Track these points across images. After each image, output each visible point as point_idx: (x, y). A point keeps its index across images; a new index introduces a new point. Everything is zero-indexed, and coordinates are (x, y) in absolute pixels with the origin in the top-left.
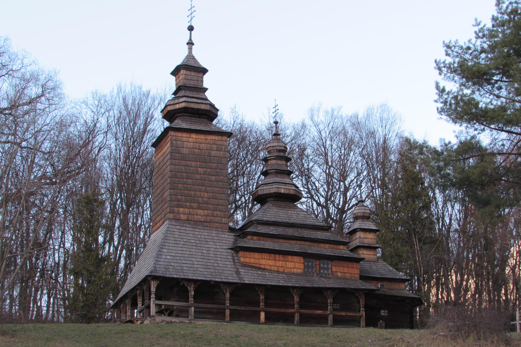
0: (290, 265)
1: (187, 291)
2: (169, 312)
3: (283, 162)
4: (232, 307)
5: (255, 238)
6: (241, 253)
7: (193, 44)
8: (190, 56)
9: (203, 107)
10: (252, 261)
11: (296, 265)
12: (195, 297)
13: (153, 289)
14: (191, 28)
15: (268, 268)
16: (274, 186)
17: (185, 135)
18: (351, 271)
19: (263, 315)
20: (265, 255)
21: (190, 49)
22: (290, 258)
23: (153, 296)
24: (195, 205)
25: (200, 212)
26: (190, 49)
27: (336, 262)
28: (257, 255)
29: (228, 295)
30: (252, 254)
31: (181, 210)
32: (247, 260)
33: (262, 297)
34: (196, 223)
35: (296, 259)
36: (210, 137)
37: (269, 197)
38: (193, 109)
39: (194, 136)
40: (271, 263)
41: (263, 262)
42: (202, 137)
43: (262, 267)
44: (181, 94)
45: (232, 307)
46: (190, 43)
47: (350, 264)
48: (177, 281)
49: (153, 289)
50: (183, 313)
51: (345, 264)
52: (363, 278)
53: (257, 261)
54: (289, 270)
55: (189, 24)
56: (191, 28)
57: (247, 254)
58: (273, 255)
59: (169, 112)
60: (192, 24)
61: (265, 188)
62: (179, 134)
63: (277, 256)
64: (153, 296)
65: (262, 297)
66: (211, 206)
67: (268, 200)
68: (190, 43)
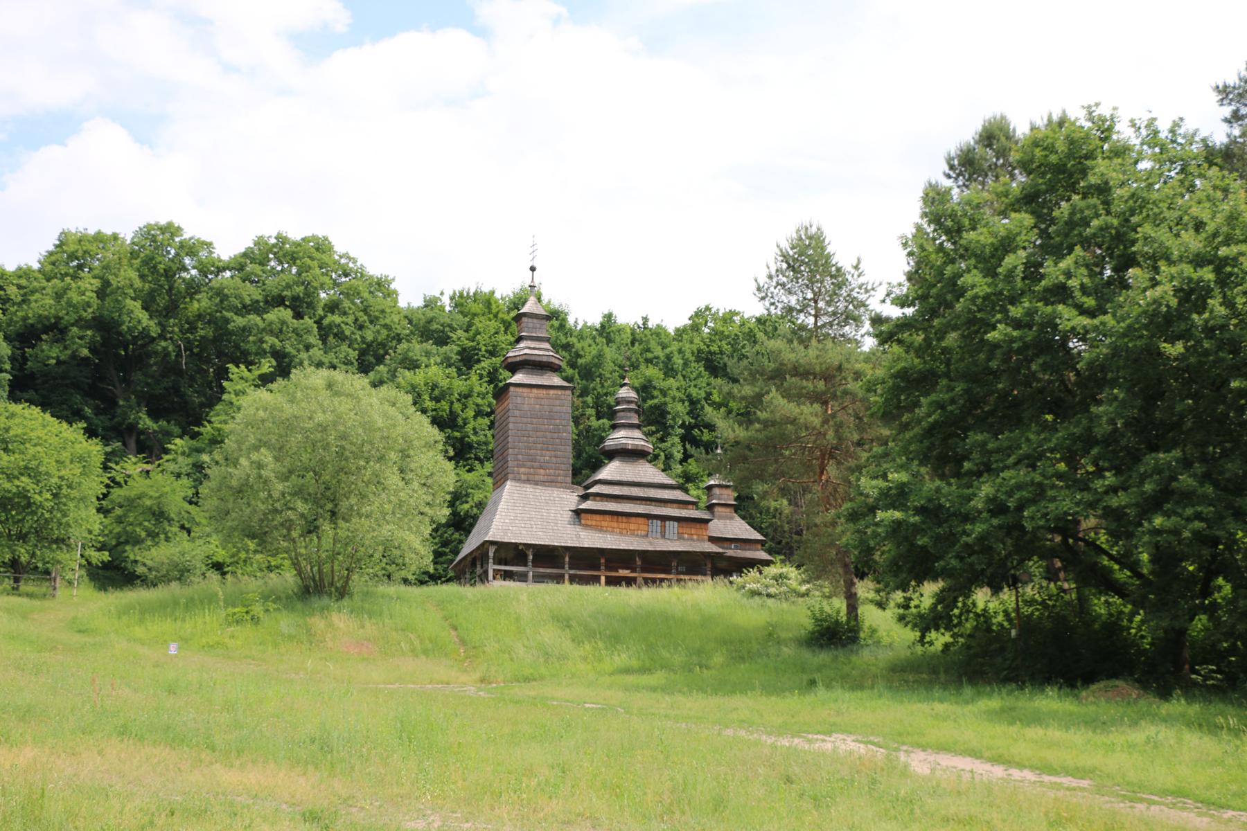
1: (526, 556)
2: (508, 576)
4: (572, 572)
6: (583, 515)
12: (533, 561)
13: (491, 554)
14: (533, 269)
19: (603, 579)
20: (608, 518)
22: (633, 519)
23: (491, 561)
24: (536, 464)
25: (542, 471)
27: (684, 524)
28: (598, 517)
29: (567, 559)
30: (594, 516)
31: (522, 470)
32: (589, 523)
33: (603, 561)
35: (640, 520)
36: (552, 392)
39: (535, 391)
42: (544, 392)
44: (522, 344)
45: (572, 572)
48: (515, 544)
49: (491, 554)
50: (522, 577)
51: (693, 525)
52: (713, 540)
56: (533, 269)
57: (589, 516)
64: (491, 561)
65: (603, 561)
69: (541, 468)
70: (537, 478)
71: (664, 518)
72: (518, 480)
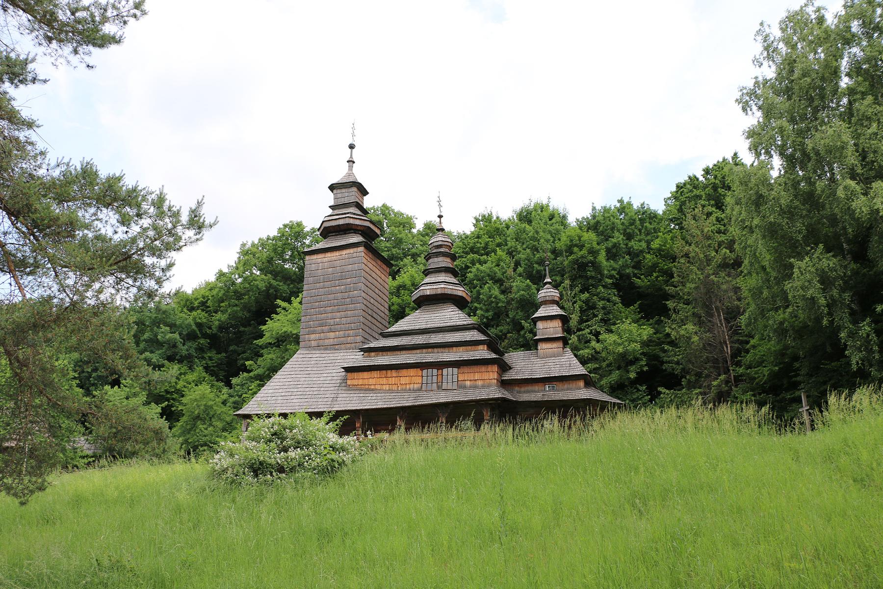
0: (404, 380)
3: (448, 260)
5: (373, 354)
8: (350, 173)
9: (341, 222)
10: (360, 382)
11: (412, 379)
14: (352, 147)
15: (378, 387)
17: (320, 256)
18: (486, 376)
20: (375, 374)
21: (351, 168)
22: (404, 372)
25: (332, 335)
26: (351, 168)
27: (465, 369)
28: (366, 375)
31: (313, 336)
32: (355, 382)
34: (326, 348)
35: (412, 372)
36: (344, 252)
40: (384, 381)
42: (337, 253)
43: (373, 387)
46: (351, 162)
47: (483, 368)
53: (366, 382)
54: (404, 387)
56: (352, 147)
58: (384, 372)
62: (314, 257)
63: (389, 371)
69: (331, 331)
70: (327, 342)
71: (440, 365)
72: (309, 347)
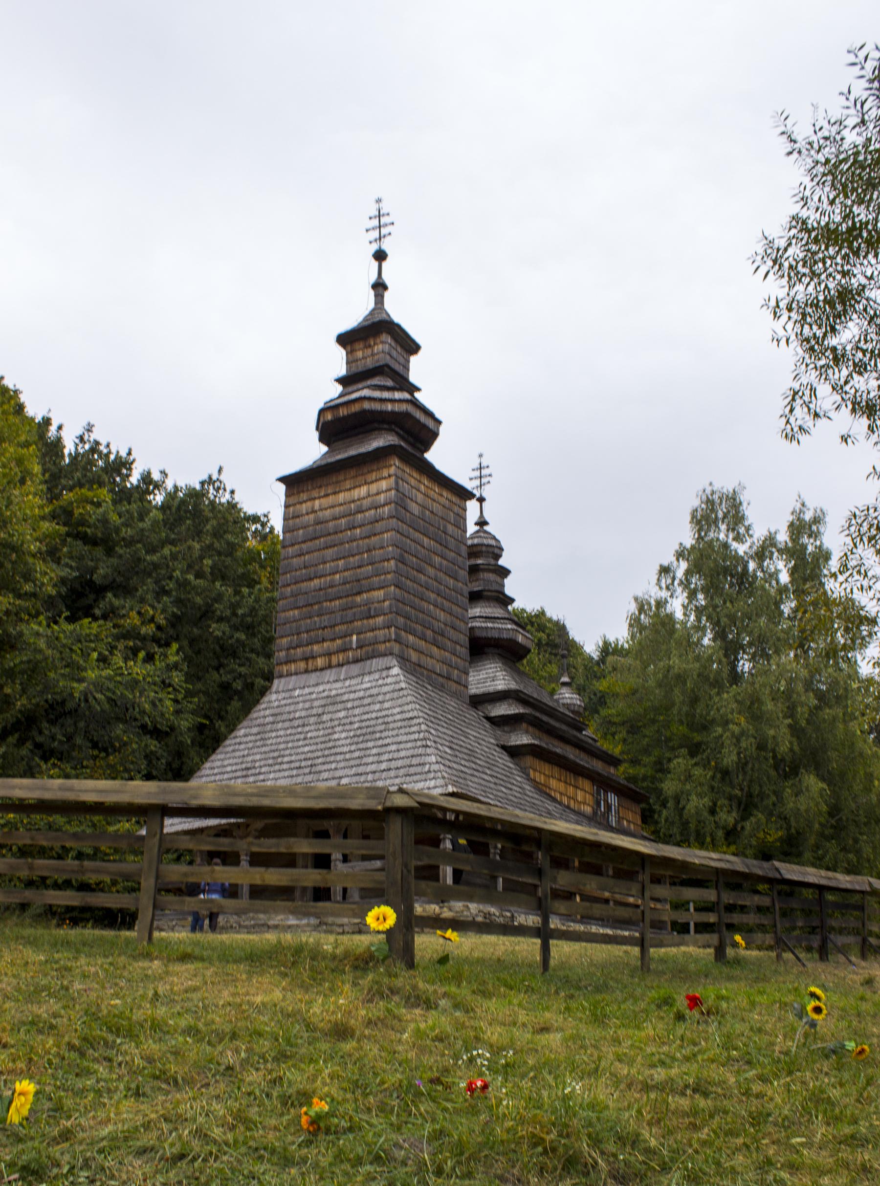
7: (385, 288)
14: (380, 256)
16: (509, 626)
28: (547, 768)
37: (489, 646)
38: (418, 421)
41: (553, 783)
46: (379, 287)
55: (375, 247)
56: (380, 256)
59: (364, 412)
60: (384, 247)
61: (490, 625)
66: (449, 643)
67: (486, 650)
68: (379, 287)
